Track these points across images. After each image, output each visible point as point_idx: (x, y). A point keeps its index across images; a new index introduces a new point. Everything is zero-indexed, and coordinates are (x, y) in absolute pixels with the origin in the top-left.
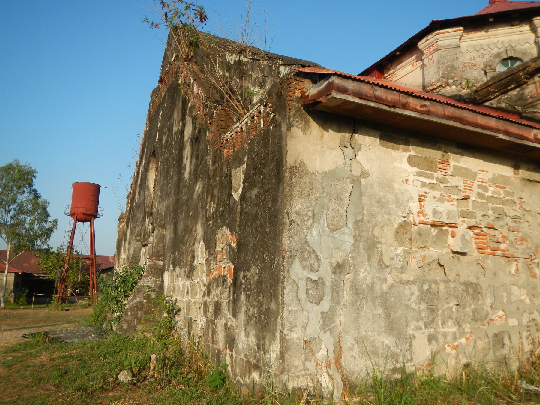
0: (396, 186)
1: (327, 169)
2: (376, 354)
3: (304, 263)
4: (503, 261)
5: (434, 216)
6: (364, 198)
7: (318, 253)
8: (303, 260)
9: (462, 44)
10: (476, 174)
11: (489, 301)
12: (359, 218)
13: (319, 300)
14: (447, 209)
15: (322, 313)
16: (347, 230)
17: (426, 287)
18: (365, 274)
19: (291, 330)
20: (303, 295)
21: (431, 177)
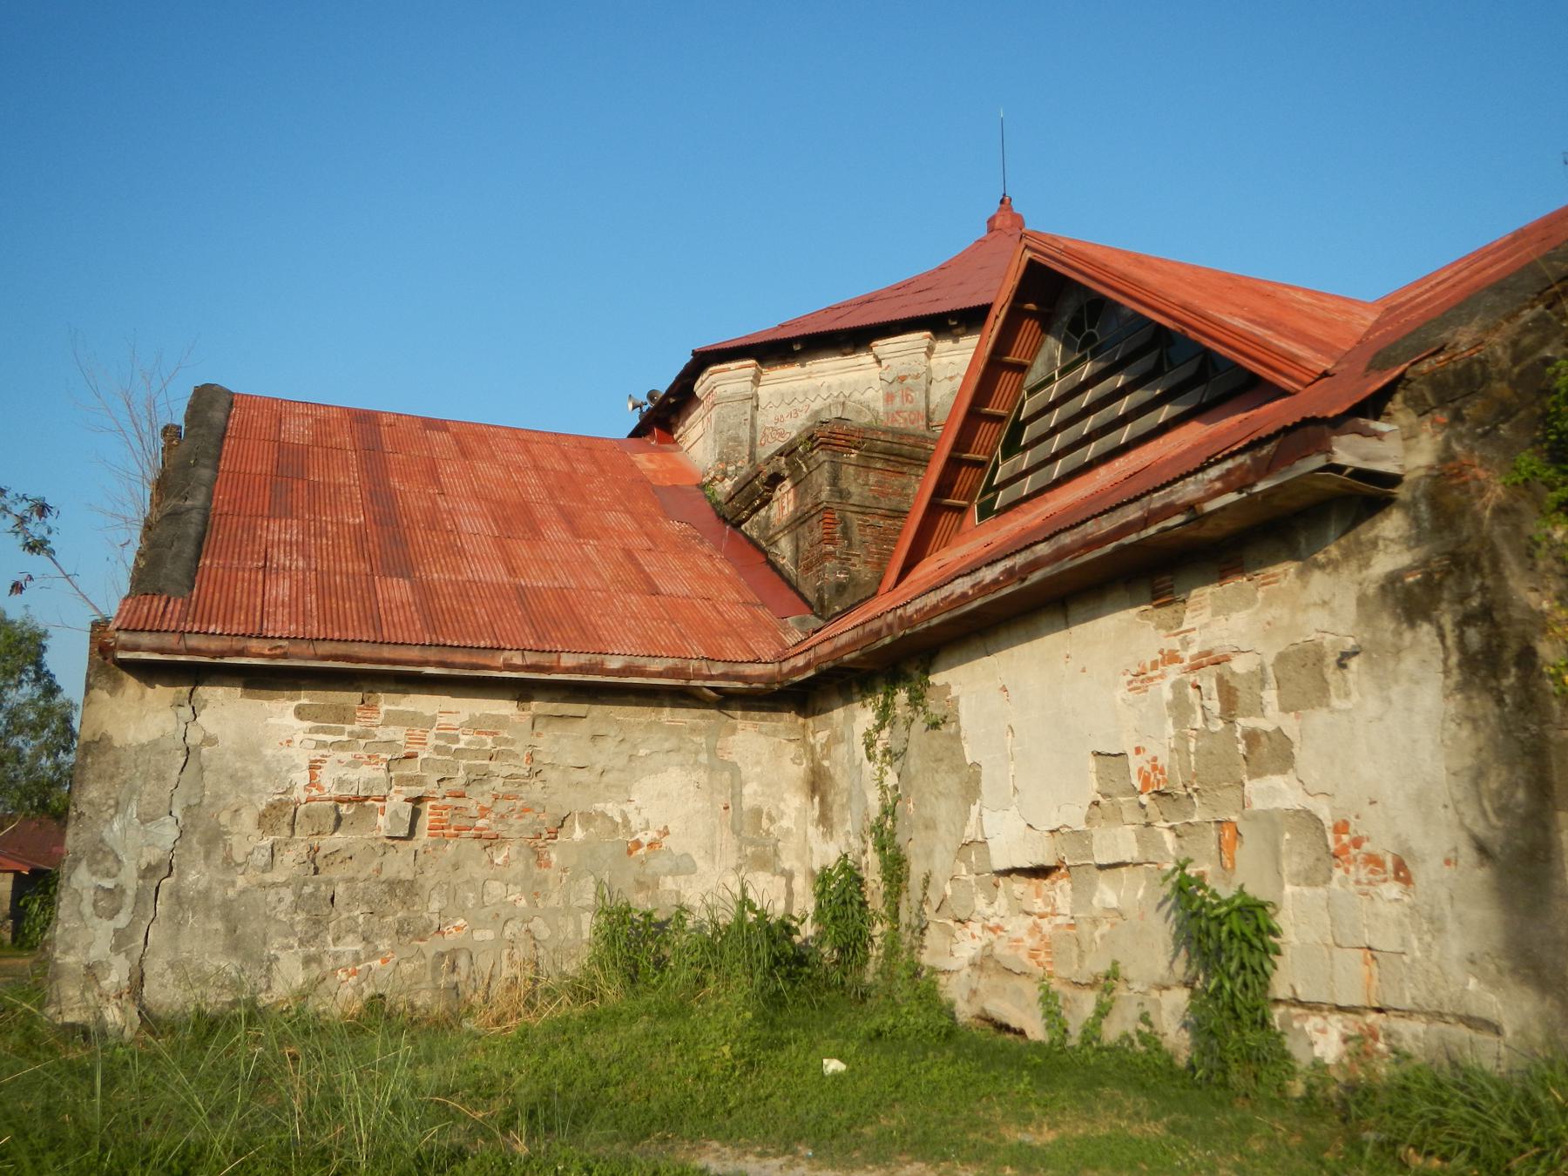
0: (268, 752)
1: (144, 739)
2: (204, 981)
3: (95, 867)
4: (477, 845)
5: (338, 788)
6: (206, 774)
7: (120, 853)
8: (93, 863)
9: (761, 391)
10: (433, 719)
11: (435, 906)
12: (194, 801)
13: (113, 914)
14: (367, 775)
15: (116, 931)
16: (169, 819)
17: (308, 890)
18: (196, 877)
19: (65, 952)
20: (87, 909)
21: (342, 732)
